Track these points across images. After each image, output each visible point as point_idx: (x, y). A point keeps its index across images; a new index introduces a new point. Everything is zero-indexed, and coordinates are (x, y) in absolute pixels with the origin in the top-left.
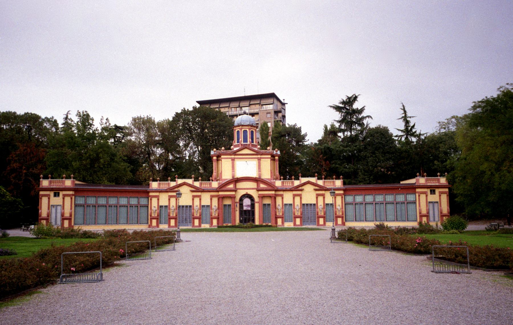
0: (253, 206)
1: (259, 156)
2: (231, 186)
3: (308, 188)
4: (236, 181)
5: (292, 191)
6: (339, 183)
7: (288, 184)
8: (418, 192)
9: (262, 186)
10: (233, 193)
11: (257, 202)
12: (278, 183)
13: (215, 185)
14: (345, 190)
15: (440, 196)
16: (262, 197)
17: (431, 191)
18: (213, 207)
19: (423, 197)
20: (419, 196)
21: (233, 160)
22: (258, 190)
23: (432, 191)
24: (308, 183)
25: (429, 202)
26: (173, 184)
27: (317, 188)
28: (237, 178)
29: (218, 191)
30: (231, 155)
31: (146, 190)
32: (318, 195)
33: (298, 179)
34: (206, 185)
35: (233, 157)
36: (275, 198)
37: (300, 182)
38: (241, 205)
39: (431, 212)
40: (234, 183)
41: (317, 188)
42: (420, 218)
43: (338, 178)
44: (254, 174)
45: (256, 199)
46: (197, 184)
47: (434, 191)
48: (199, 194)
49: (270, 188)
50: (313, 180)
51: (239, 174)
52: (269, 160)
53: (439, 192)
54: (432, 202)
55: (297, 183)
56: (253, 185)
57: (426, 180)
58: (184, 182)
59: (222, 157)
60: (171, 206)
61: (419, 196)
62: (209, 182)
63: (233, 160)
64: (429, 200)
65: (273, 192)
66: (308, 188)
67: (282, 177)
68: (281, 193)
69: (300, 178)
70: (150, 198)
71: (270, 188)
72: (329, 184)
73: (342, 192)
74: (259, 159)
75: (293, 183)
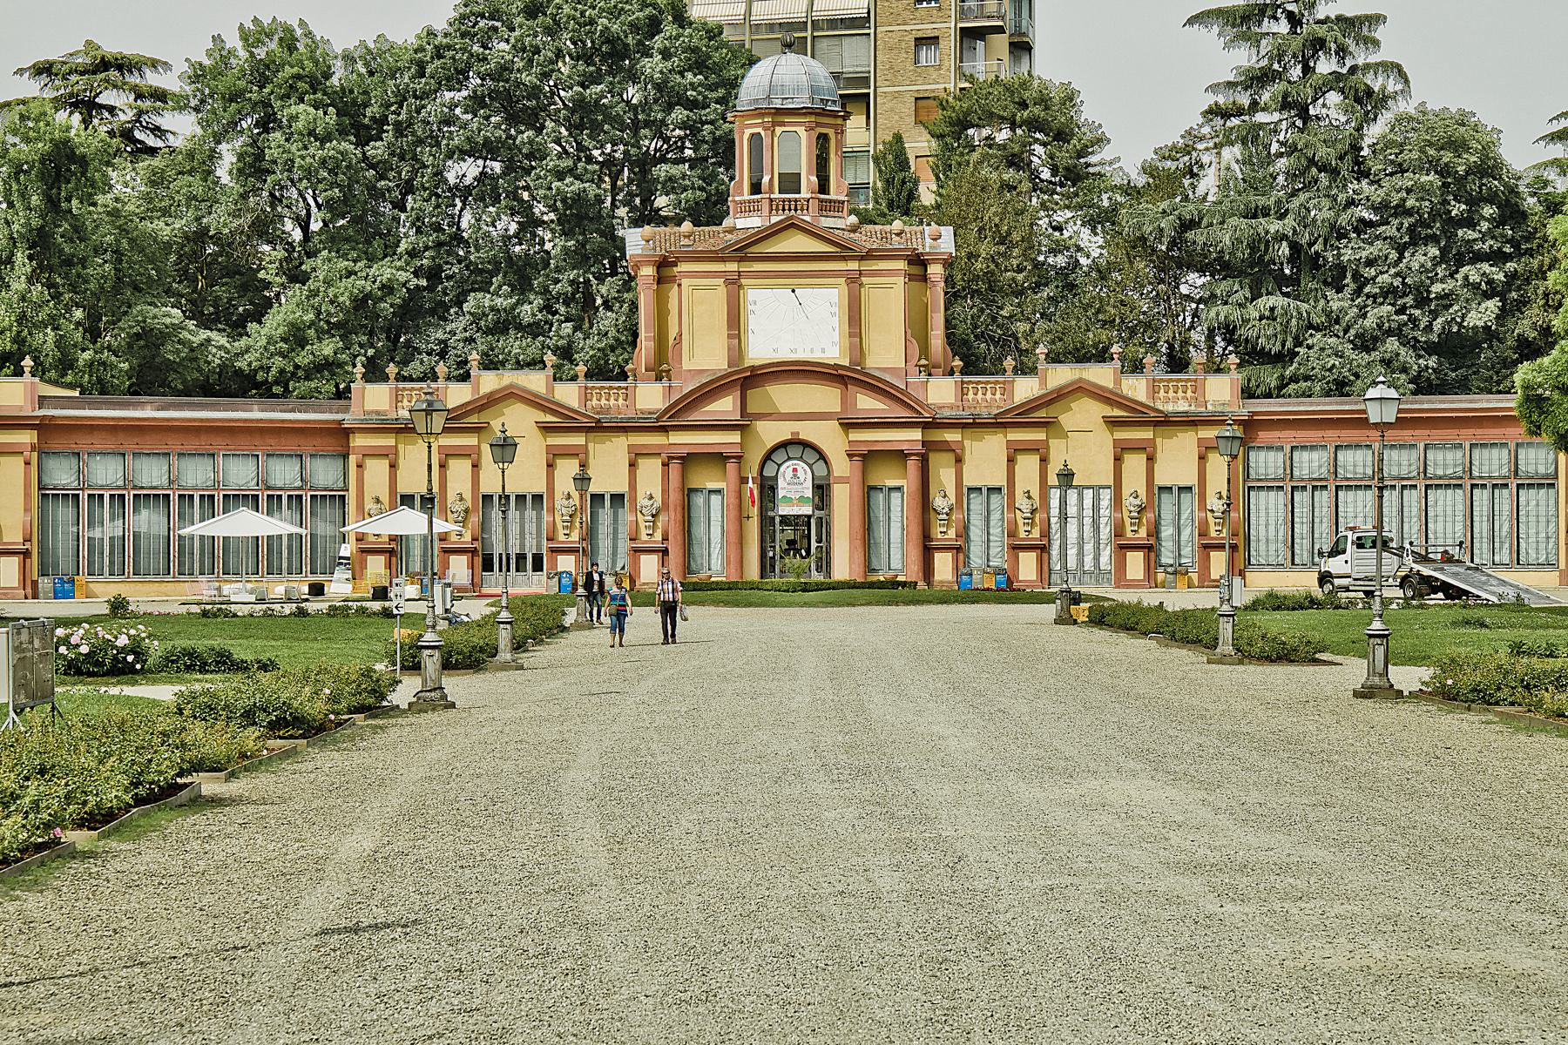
0: (822, 491)
1: (854, 265)
2: (725, 406)
3: (1084, 415)
4: (749, 379)
5: (1004, 425)
7: (987, 396)
9: (867, 404)
10: (735, 437)
11: (842, 480)
12: (941, 393)
13: (650, 397)
16: (867, 458)
18: (642, 501)
21: (734, 284)
22: (848, 425)
24: (1080, 389)
26: (457, 395)
27: (1117, 412)
28: (753, 368)
29: (664, 429)
30: (723, 260)
31: (340, 422)
32: (1121, 451)
34: (608, 400)
35: (732, 267)
36: (924, 461)
37: (1044, 382)
41: (1117, 412)
44: (830, 349)
45: (841, 466)
46: (568, 394)
48: (578, 440)
49: (901, 413)
50: (1100, 375)
51: (759, 351)
52: (901, 280)
54: (1092, 487)
55: (1026, 389)
56: (826, 397)
58: (511, 386)
59: (683, 267)
60: (451, 496)
62: (623, 384)
63: (734, 284)
65: (916, 435)
66: (1084, 415)
67: (958, 363)
68: (952, 436)
70: (353, 459)
71: (901, 413)
74: (854, 280)
75: (1007, 389)
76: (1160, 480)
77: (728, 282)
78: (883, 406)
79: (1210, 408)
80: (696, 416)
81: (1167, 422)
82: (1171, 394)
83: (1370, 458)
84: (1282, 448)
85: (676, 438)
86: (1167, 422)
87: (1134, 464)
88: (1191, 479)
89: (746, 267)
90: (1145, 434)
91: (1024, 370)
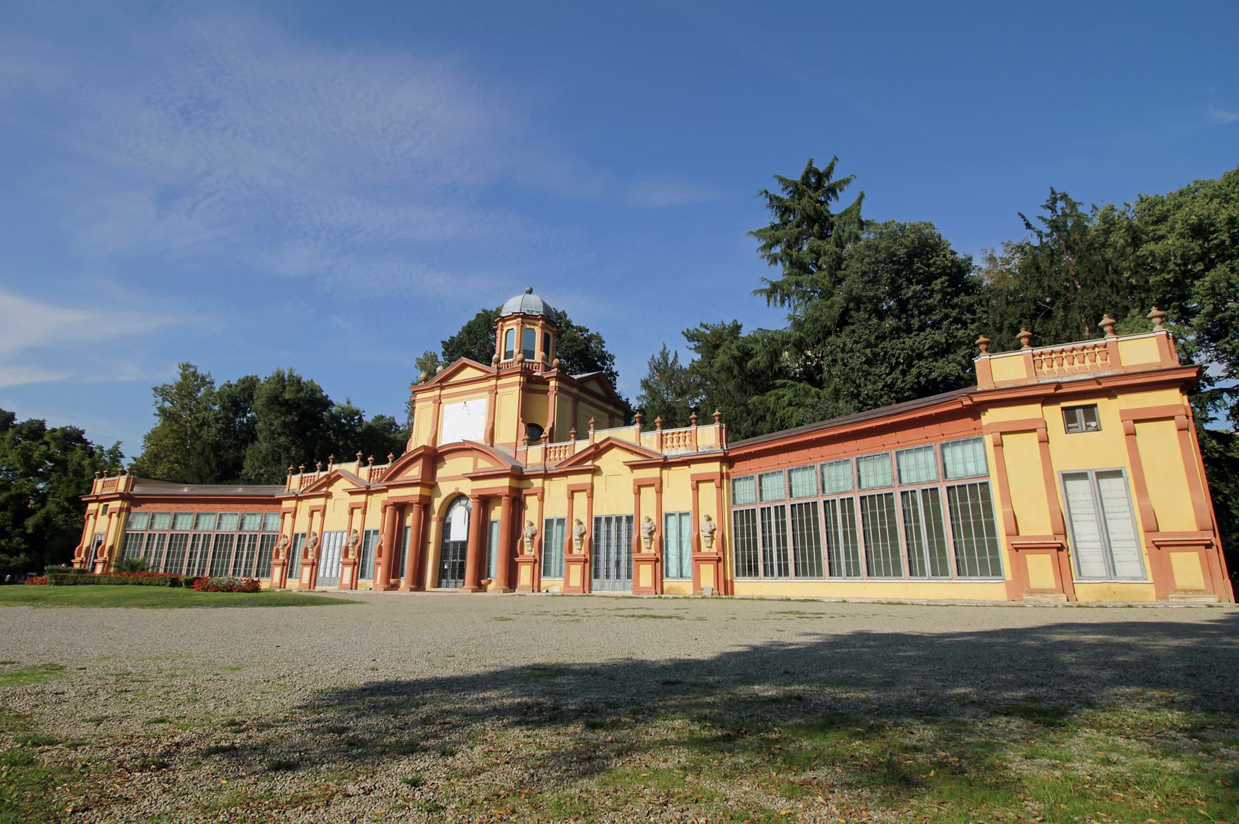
1: (493, 382)
6: (708, 437)
8: (991, 428)
14: (728, 460)
15: (1131, 434)
17: (1069, 414)
19: (1021, 449)
20: (999, 445)
23: (1080, 413)
25: (1067, 477)
33: (587, 437)
35: (437, 392)
38: (445, 528)
39: (1085, 532)
40: (421, 461)
42: (1012, 558)
43: (705, 420)
47: (1090, 412)
51: (445, 439)
53: (1122, 412)
57: (1035, 362)
61: (999, 445)
63: (438, 402)
64: (1061, 464)
65: (505, 482)
69: (591, 432)
72: (677, 443)
73: (715, 467)
76: (666, 509)
77: (435, 402)
78: (491, 466)
79: (700, 450)
80: (399, 479)
81: (666, 464)
82: (675, 443)
83: (814, 478)
84: (752, 478)
85: (393, 493)
86: (666, 464)
87: (648, 494)
88: (688, 506)
89: (444, 392)
90: (654, 473)
91: (578, 437)
